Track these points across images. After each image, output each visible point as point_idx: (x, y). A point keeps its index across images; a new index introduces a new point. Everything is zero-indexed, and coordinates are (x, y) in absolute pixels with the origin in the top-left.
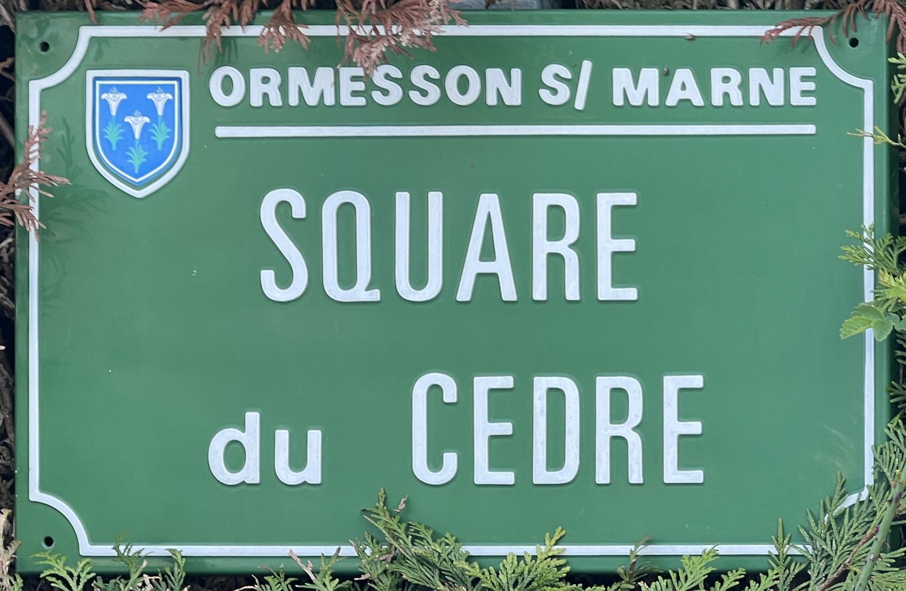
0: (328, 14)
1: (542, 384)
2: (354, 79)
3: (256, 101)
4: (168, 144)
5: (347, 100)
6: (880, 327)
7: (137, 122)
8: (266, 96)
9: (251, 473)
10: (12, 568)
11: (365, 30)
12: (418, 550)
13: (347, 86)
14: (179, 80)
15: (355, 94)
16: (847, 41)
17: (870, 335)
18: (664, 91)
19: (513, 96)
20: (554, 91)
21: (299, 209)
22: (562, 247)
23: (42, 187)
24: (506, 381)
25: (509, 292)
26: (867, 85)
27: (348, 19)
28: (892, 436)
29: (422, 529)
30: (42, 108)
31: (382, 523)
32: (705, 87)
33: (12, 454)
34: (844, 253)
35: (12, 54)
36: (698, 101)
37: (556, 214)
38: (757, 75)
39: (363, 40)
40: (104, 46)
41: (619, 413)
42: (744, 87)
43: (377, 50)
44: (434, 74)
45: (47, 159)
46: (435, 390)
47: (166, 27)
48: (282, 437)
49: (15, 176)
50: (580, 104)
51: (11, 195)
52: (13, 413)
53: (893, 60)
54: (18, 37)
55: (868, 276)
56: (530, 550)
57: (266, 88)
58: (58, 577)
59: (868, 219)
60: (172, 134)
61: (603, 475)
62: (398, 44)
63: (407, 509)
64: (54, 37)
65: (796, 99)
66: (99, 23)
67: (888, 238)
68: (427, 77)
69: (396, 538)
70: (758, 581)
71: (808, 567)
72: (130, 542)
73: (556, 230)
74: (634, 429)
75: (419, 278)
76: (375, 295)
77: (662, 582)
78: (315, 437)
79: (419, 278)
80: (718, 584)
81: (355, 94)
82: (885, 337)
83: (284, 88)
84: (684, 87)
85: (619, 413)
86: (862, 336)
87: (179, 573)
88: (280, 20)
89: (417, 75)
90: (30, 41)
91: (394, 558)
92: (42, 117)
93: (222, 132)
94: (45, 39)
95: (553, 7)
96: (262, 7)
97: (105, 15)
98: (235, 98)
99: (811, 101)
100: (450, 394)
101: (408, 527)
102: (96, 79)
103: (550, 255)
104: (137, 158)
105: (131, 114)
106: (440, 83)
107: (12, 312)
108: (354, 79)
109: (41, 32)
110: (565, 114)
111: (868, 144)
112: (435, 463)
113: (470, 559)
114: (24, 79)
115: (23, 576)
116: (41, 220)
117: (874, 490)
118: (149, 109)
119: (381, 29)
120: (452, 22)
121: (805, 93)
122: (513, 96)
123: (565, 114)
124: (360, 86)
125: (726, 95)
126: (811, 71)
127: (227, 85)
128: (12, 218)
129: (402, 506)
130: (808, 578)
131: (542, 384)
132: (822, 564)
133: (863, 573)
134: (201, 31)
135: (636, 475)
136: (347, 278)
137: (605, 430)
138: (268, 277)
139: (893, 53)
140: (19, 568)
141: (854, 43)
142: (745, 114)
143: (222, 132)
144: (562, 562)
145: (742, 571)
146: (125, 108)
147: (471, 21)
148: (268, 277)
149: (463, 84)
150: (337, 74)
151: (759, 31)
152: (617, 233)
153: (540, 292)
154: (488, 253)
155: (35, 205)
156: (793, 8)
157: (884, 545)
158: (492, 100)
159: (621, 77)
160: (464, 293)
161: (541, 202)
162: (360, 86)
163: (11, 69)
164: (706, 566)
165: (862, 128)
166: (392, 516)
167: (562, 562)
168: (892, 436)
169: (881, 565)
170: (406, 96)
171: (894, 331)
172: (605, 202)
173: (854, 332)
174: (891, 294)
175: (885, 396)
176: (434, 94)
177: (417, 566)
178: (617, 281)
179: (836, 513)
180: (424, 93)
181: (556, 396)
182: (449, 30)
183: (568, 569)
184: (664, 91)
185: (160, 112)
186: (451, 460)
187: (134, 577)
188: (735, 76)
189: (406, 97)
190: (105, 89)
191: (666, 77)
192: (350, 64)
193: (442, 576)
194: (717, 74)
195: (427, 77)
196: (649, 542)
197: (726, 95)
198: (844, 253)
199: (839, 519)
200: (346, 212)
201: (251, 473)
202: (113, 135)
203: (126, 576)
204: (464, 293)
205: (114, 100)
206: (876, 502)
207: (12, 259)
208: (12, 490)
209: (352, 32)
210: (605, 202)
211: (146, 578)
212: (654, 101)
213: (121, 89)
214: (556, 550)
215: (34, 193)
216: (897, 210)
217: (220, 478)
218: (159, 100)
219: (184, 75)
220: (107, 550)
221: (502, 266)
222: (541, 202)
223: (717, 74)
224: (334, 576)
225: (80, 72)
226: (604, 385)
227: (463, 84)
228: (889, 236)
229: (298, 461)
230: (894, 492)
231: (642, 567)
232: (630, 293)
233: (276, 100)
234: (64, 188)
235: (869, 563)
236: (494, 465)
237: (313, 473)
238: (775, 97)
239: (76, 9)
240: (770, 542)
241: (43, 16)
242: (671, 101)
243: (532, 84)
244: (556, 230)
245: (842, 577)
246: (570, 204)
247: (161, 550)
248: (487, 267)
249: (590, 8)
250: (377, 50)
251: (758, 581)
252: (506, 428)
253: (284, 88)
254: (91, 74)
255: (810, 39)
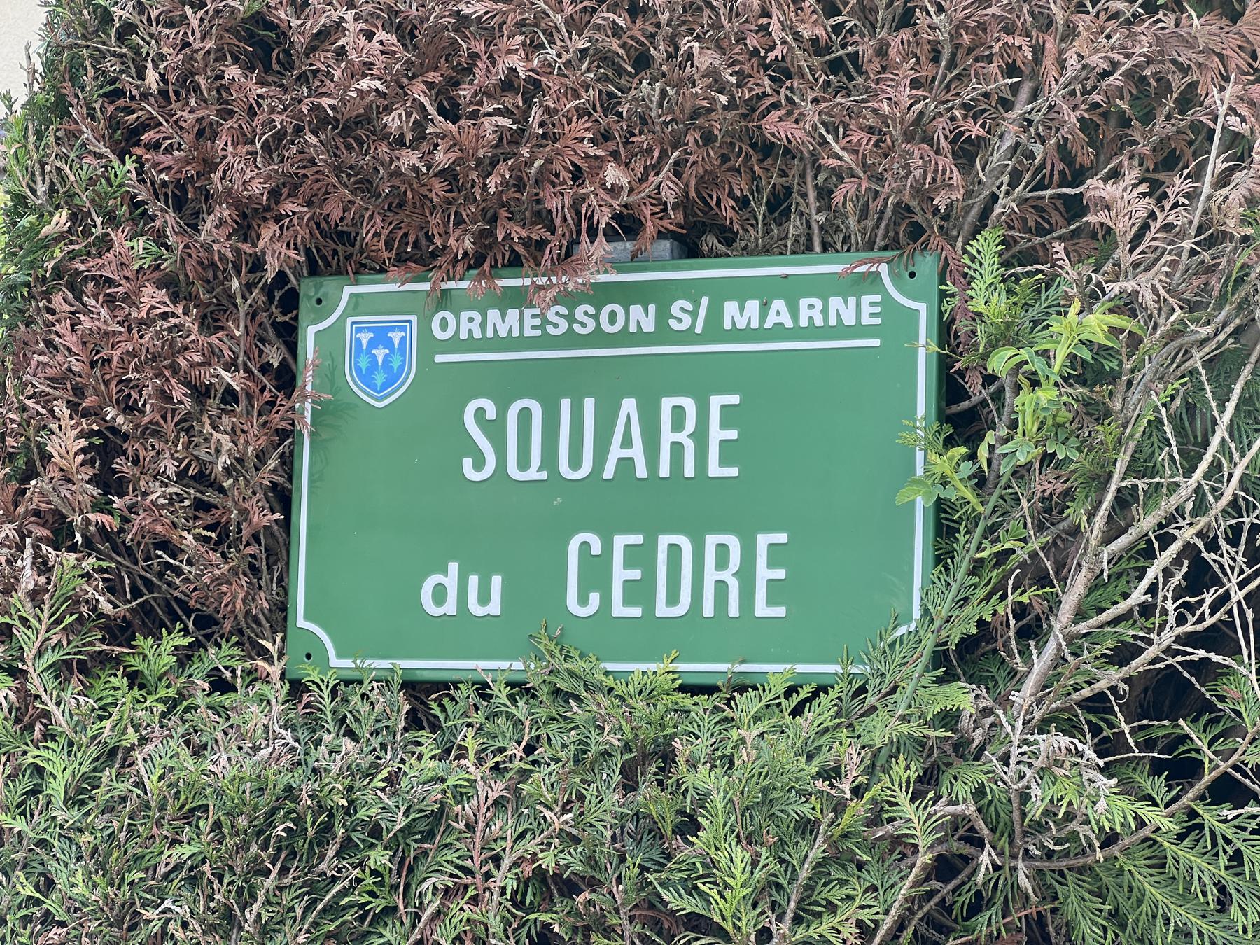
0: (517, 270)
1: (664, 541)
2: (534, 316)
3: (464, 335)
4: (401, 368)
5: (528, 332)
6: (927, 495)
7: (380, 353)
8: (470, 331)
9: (450, 607)
10: (283, 675)
11: (543, 281)
12: (569, 666)
13: (528, 322)
14: (410, 322)
15: (534, 327)
16: (907, 274)
17: (920, 502)
18: (763, 316)
19: (649, 325)
20: (680, 320)
21: (491, 414)
22: (682, 437)
23: (313, 402)
24: (637, 539)
25: (641, 471)
26: (922, 307)
27: (530, 273)
28: (936, 580)
29: (572, 650)
30: (315, 346)
31: (544, 645)
32: (795, 313)
33: (286, 594)
34: (900, 438)
35: (297, 308)
36: (789, 323)
37: (679, 412)
38: (836, 303)
39: (541, 288)
40: (360, 300)
41: (722, 563)
42: (825, 312)
43: (551, 294)
44: (592, 310)
45: (318, 382)
46: (585, 545)
47: (403, 284)
48: (474, 580)
49: (296, 394)
50: (698, 330)
51: (293, 408)
52: (288, 564)
53: (943, 287)
54: (301, 295)
55: (920, 456)
56: (651, 667)
57: (471, 326)
58: (314, 683)
59: (921, 411)
60: (404, 361)
61: (708, 610)
62: (566, 289)
63: (562, 635)
64: (326, 294)
65: (866, 320)
66: (356, 283)
67: (936, 426)
68: (586, 313)
69: (553, 657)
70: (827, 693)
71: (866, 683)
72: (364, 658)
73: (678, 425)
74: (734, 575)
75: (575, 463)
76: (543, 475)
77: (751, 692)
78: (497, 581)
79: (575, 463)
80: (795, 695)
81: (534, 327)
82: (931, 503)
83: (483, 326)
84: (778, 313)
85: (722, 563)
86: (914, 502)
87: (398, 681)
88: (483, 275)
89: (579, 313)
90: (309, 298)
91: (551, 672)
92: (315, 352)
93: (439, 358)
94: (319, 296)
95: (681, 258)
96: (470, 267)
97: (361, 277)
98: (449, 333)
99: (878, 321)
100: (596, 549)
101: (562, 648)
102: (353, 323)
103: (673, 443)
104: (380, 379)
105: (376, 348)
106: (596, 317)
107: (290, 491)
108: (534, 316)
109: (316, 293)
110: (688, 336)
111: (922, 353)
112: (583, 600)
113: (607, 673)
114: (305, 325)
115: (290, 681)
116: (312, 425)
117: (921, 623)
118: (389, 343)
119: (554, 280)
120: (606, 272)
121: (872, 315)
122: (649, 325)
123: (688, 336)
124: (538, 322)
125: (811, 318)
126: (878, 298)
127: (444, 325)
128: (293, 424)
129: (558, 633)
130: (867, 691)
131: (664, 541)
132: (878, 681)
133: (910, 688)
134: (426, 286)
135: (734, 610)
136: (524, 464)
137: (711, 575)
138: (467, 463)
139: (943, 281)
140: (288, 676)
141: (912, 275)
142: (826, 332)
143: (439, 358)
144: (676, 676)
145: (814, 685)
146: (373, 344)
147: (619, 271)
148: (467, 463)
149: (613, 318)
150: (521, 313)
151: (838, 269)
152: (724, 425)
153: (665, 472)
154: (627, 442)
155: (308, 415)
156: (864, 250)
157: (927, 666)
158: (633, 329)
159: (731, 307)
160: (609, 473)
161: (667, 404)
162: (538, 322)
163: (296, 318)
164: (787, 681)
165: (917, 340)
166: (551, 640)
167: (676, 676)
168: (936, 580)
169: (924, 682)
170: (570, 328)
171: (939, 499)
172: (716, 402)
173: (907, 500)
174: (936, 470)
175: (931, 549)
176: (591, 325)
177: (568, 678)
178: (723, 462)
179: (890, 640)
180: (584, 325)
181: (674, 549)
182: (603, 278)
183: (680, 682)
184: (763, 316)
185: (396, 346)
186: (595, 598)
187: (366, 683)
188: (818, 303)
189: (570, 328)
190: (359, 330)
191: (765, 306)
192: (531, 306)
193: (586, 685)
194: (804, 303)
195: (586, 313)
196: (743, 662)
197: (811, 318)
198: (900, 438)
199: (892, 645)
200: (525, 414)
201: (450, 607)
202: (364, 363)
203: (361, 683)
204: (609, 473)
205: (365, 338)
206: (921, 633)
207: (292, 453)
208: (285, 619)
209: (533, 283)
210: (716, 402)
211: (374, 684)
212: (477, 334)
213: (370, 330)
214: (671, 667)
215: (308, 406)
216: (944, 404)
217: (428, 611)
218: (396, 337)
219: (414, 318)
220: (348, 663)
221: (637, 452)
222: (667, 404)
223: (804, 303)
224: (507, 684)
225: (343, 318)
226: (711, 541)
227: (613, 318)
228: (937, 424)
229: (484, 599)
230: (936, 625)
231: (735, 681)
232: (733, 472)
233: (477, 334)
234: (329, 402)
235: (915, 681)
236: (627, 602)
237: (494, 608)
238: (849, 319)
239: (340, 273)
240: (837, 663)
241: (319, 280)
242: (768, 325)
243: (664, 315)
244: (678, 425)
245: (893, 691)
246: (689, 404)
247: (386, 663)
248: (626, 453)
249: (709, 257)
250: (551, 294)
251: (827, 693)
252: (636, 574)
253: (483, 326)
254: (350, 320)
255: (878, 274)
